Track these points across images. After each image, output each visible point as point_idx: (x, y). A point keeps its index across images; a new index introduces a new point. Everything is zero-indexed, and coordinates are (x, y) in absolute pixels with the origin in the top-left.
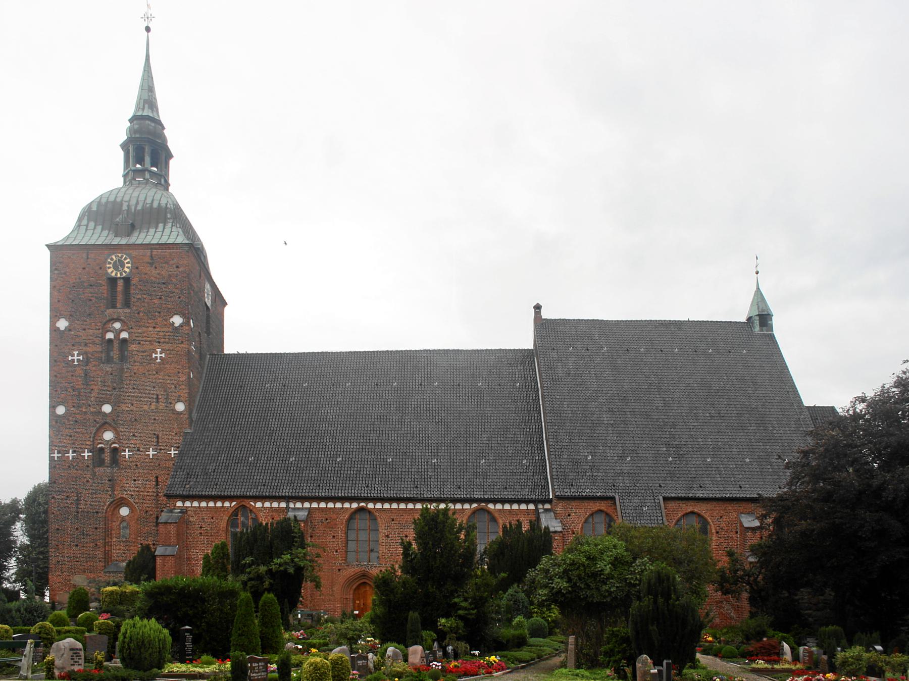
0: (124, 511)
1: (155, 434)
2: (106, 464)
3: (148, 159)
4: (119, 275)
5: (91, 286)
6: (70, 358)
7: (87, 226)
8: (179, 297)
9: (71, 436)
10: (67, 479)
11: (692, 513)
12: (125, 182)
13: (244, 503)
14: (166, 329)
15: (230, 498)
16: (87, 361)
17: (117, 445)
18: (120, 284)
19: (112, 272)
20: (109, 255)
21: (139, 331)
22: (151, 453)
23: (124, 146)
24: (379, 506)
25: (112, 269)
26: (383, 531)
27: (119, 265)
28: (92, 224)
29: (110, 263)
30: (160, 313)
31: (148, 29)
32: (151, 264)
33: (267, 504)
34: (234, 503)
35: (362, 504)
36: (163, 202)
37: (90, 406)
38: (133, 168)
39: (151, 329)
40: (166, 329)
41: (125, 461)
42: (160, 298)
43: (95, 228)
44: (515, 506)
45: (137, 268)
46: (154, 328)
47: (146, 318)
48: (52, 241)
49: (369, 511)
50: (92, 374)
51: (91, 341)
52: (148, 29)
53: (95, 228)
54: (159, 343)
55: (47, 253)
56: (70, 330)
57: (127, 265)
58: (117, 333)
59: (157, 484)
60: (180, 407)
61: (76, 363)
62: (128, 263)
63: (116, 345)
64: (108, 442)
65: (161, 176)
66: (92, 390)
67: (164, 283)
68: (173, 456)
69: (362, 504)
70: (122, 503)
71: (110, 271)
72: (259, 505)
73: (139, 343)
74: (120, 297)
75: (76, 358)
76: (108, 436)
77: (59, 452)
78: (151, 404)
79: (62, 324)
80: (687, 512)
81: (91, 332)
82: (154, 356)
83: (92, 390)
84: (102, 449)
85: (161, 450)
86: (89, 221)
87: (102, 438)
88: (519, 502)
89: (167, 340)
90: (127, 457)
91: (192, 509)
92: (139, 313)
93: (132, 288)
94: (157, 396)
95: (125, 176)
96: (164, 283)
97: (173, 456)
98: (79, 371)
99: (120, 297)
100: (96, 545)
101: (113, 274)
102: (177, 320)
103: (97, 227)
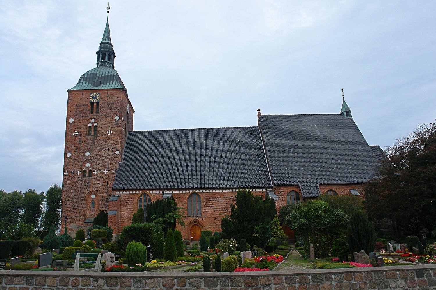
0: (93, 196)
1: (107, 164)
3: (106, 58)
4: (95, 101)
5: (83, 105)
6: (74, 134)
7: (83, 83)
8: (118, 109)
9: (72, 166)
10: (70, 183)
11: (331, 190)
12: (97, 66)
13: (145, 192)
14: (112, 122)
15: (139, 190)
16: (80, 135)
17: (91, 169)
18: (95, 104)
20: (91, 94)
21: (102, 122)
22: (105, 172)
23: (98, 53)
24: (201, 191)
25: (92, 99)
26: (203, 202)
28: (85, 82)
29: (91, 96)
30: (110, 115)
31: (108, 12)
32: (108, 97)
33: (154, 192)
34: (140, 192)
35: (194, 191)
36: (112, 74)
37: (81, 153)
38: (101, 61)
39: (106, 122)
40: (112, 122)
41: (94, 175)
42: (111, 110)
43: (86, 83)
44: (257, 190)
45: (102, 98)
46: (108, 121)
47: (105, 117)
49: (197, 194)
50: (82, 140)
51: (82, 127)
52: (108, 12)
53: (86, 83)
54: (110, 127)
56: (74, 123)
57: (98, 97)
58: (93, 123)
59: (107, 185)
60: (118, 153)
61: (76, 136)
62: (98, 96)
63: (92, 129)
64: (87, 167)
65: (111, 64)
66: (82, 146)
67: (112, 104)
68: (114, 173)
69: (194, 191)
70: (92, 193)
71: (91, 99)
72: (151, 192)
73: (102, 127)
74: (95, 110)
75: (76, 134)
76: (88, 165)
77: (67, 172)
78: (106, 152)
79: (71, 120)
80: (329, 190)
81: (83, 123)
82: (107, 132)
83: (82, 146)
84: (85, 171)
85: (109, 170)
86: (83, 81)
87: (85, 166)
88: (259, 188)
89: (113, 126)
90: (95, 174)
91: (123, 195)
92: (102, 116)
93: (100, 106)
94: (108, 148)
95: (97, 64)
96: (112, 104)
97: (114, 173)
98: (77, 139)
99: (95, 110)
100: (81, 211)
101: (92, 101)
102: (117, 118)
103: (87, 83)
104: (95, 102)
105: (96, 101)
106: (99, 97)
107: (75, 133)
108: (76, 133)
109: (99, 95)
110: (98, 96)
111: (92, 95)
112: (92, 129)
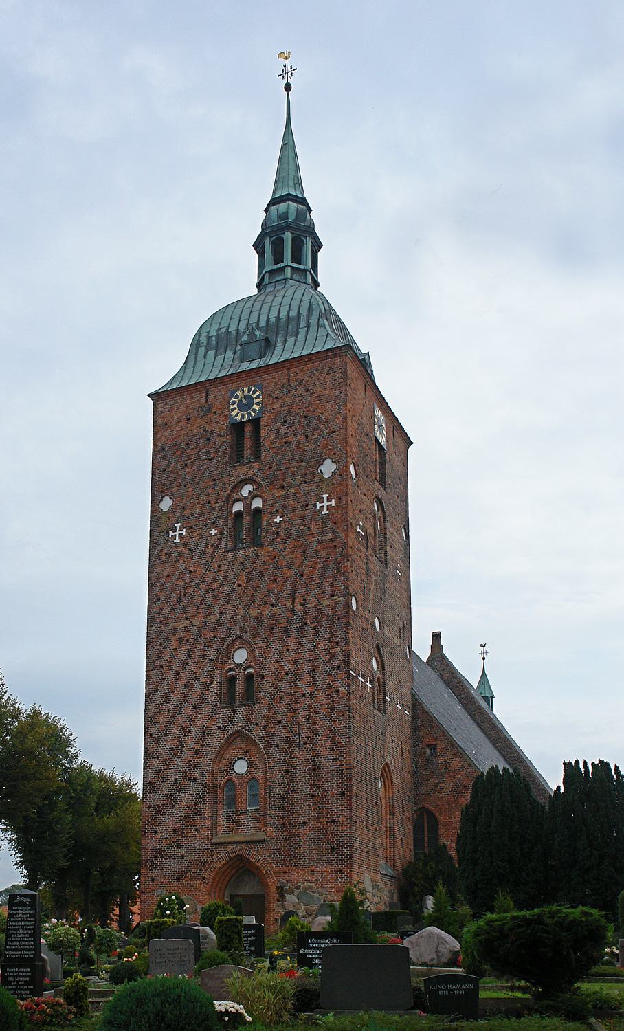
2: (238, 703)
4: (246, 418)
12: (259, 291)
19: (236, 415)
23: (258, 246)
25: (236, 411)
27: (246, 405)
29: (234, 403)
48: (158, 384)
55: (150, 402)
57: (256, 401)
58: (247, 501)
62: (258, 397)
63: (246, 519)
65: (304, 271)
95: (259, 286)
104: (247, 421)
105: (249, 415)
106: (259, 400)
107: (175, 530)
108: (178, 529)
109: (258, 393)
110: (258, 397)
111: (237, 397)
112: (246, 519)
